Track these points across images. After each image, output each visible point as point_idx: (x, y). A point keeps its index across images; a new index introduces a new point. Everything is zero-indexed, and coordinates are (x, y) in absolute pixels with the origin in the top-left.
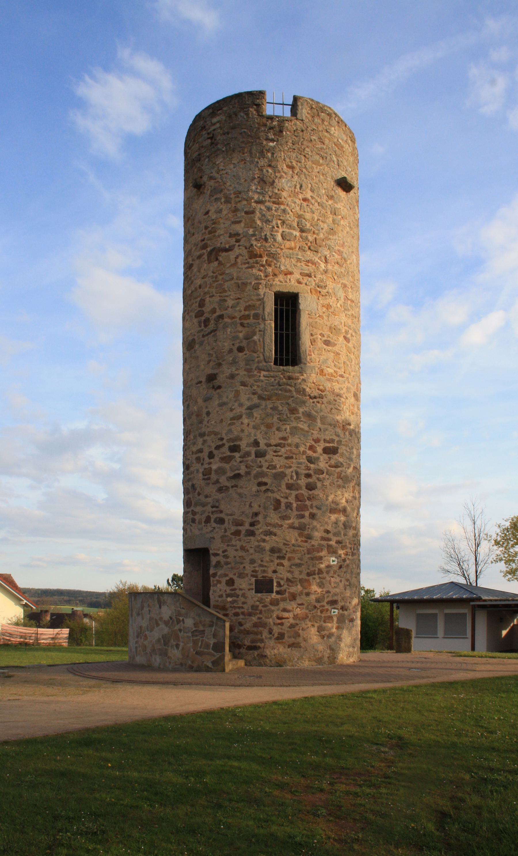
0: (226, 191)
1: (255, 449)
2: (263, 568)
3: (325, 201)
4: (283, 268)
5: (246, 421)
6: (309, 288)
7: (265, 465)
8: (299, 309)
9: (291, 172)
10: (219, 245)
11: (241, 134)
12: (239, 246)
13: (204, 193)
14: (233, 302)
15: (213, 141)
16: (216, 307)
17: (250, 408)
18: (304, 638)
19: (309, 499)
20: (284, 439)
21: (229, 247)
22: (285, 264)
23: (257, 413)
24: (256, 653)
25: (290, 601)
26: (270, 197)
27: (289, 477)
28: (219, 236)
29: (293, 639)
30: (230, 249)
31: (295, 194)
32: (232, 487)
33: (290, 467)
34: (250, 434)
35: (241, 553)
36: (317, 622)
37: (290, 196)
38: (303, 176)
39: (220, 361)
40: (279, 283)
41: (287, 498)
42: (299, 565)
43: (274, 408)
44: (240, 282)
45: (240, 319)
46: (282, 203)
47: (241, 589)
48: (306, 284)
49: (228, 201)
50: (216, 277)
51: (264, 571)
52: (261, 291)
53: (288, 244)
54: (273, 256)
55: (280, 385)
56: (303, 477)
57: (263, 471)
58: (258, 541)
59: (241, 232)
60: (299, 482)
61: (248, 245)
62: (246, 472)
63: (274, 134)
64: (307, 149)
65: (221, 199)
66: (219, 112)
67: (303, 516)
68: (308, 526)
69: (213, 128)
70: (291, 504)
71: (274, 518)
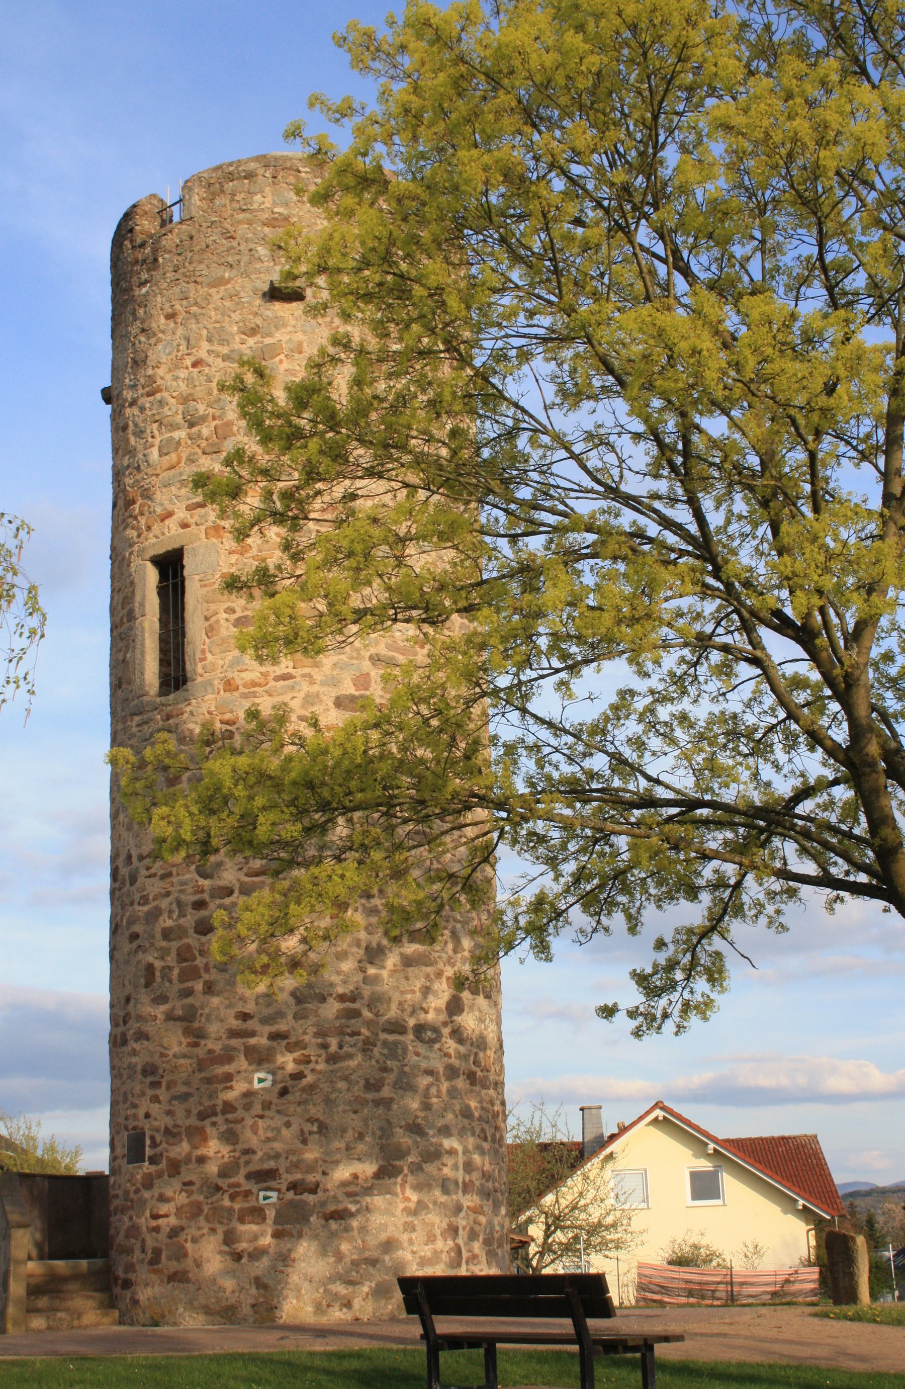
3: (237, 346)
4: (159, 510)
6: (203, 528)
9: (172, 325)
18: (195, 1260)
25: (170, 1176)
29: (175, 1263)
31: (177, 364)
33: (168, 894)
36: (222, 1223)
37: (170, 371)
38: (193, 321)
40: (154, 540)
42: (184, 1097)
48: (197, 524)
54: (147, 494)
56: (189, 910)
60: (182, 921)
63: (149, 270)
67: (189, 993)
68: (200, 1012)
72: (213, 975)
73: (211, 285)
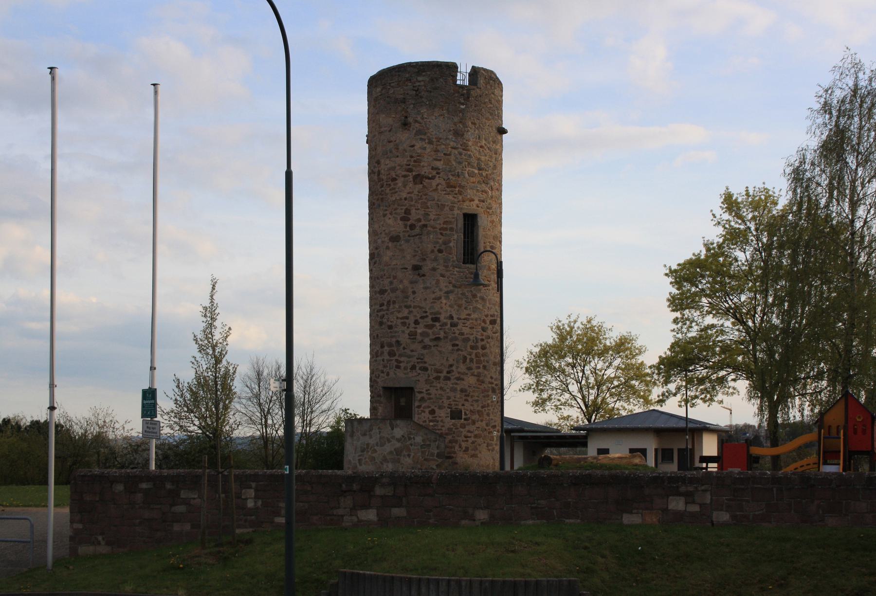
0: (429, 135)
1: (450, 321)
2: (455, 403)
4: (469, 196)
5: (444, 301)
7: (457, 332)
8: (478, 225)
10: (423, 173)
11: (441, 95)
12: (439, 177)
13: (409, 130)
14: (434, 217)
15: (418, 93)
16: (422, 218)
17: (447, 293)
19: (483, 356)
20: (469, 315)
21: (432, 176)
22: (470, 193)
23: (452, 296)
24: (451, 460)
26: (461, 145)
27: (472, 341)
28: (423, 167)
30: (433, 178)
32: (434, 346)
33: (472, 334)
34: (447, 310)
35: (440, 392)
37: (473, 145)
39: (425, 257)
40: (466, 207)
41: (470, 355)
42: (477, 401)
43: (463, 294)
44: (439, 203)
45: (440, 229)
46: (468, 150)
47: (440, 417)
49: (430, 142)
50: (421, 196)
51: (457, 405)
52: (456, 212)
53: (472, 179)
55: (466, 278)
57: (456, 336)
58: (452, 384)
59: (441, 168)
61: (446, 178)
62: (444, 337)
63: (464, 100)
64: (483, 110)
65: (425, 140)
66: (424, 74)
67: (479, 368)
69: (418, 84)
70: (473, 359)
71: (462, 368)
72: (486, 364)
73: (486, 119)
